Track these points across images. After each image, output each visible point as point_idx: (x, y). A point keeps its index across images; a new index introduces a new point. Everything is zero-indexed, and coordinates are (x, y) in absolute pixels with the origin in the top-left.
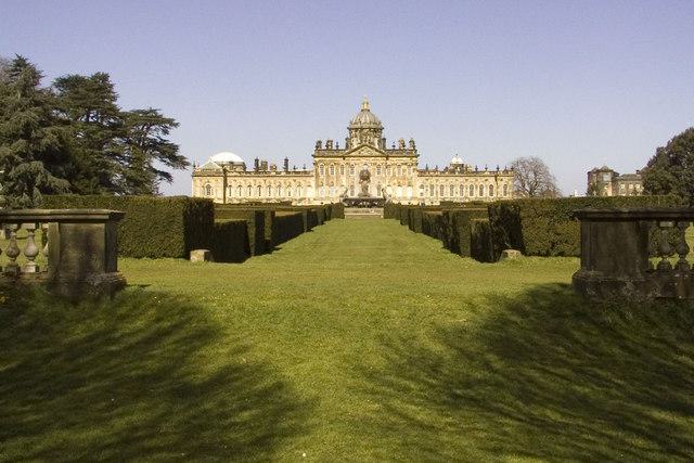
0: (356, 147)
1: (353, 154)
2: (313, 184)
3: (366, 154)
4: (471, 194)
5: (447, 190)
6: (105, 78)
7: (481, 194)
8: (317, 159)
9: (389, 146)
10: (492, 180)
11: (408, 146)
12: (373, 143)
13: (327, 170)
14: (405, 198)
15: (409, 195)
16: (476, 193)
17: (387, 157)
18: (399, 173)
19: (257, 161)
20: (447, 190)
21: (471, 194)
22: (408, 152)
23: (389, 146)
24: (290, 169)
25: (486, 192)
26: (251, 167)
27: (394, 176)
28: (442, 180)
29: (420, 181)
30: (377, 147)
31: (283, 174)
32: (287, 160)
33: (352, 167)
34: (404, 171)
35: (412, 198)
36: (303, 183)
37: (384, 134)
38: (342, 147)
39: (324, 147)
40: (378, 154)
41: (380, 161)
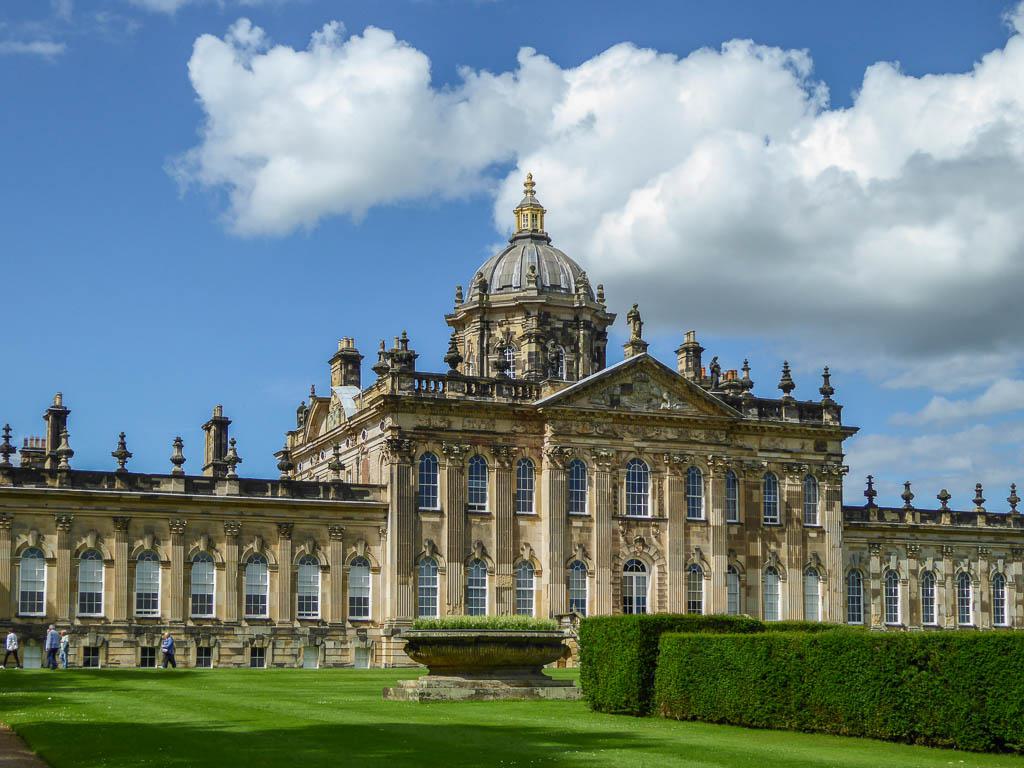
1: (583, 403)
3: (643, 409)
8: (409, 422)
17: (735, 428)
40: (690, 411)
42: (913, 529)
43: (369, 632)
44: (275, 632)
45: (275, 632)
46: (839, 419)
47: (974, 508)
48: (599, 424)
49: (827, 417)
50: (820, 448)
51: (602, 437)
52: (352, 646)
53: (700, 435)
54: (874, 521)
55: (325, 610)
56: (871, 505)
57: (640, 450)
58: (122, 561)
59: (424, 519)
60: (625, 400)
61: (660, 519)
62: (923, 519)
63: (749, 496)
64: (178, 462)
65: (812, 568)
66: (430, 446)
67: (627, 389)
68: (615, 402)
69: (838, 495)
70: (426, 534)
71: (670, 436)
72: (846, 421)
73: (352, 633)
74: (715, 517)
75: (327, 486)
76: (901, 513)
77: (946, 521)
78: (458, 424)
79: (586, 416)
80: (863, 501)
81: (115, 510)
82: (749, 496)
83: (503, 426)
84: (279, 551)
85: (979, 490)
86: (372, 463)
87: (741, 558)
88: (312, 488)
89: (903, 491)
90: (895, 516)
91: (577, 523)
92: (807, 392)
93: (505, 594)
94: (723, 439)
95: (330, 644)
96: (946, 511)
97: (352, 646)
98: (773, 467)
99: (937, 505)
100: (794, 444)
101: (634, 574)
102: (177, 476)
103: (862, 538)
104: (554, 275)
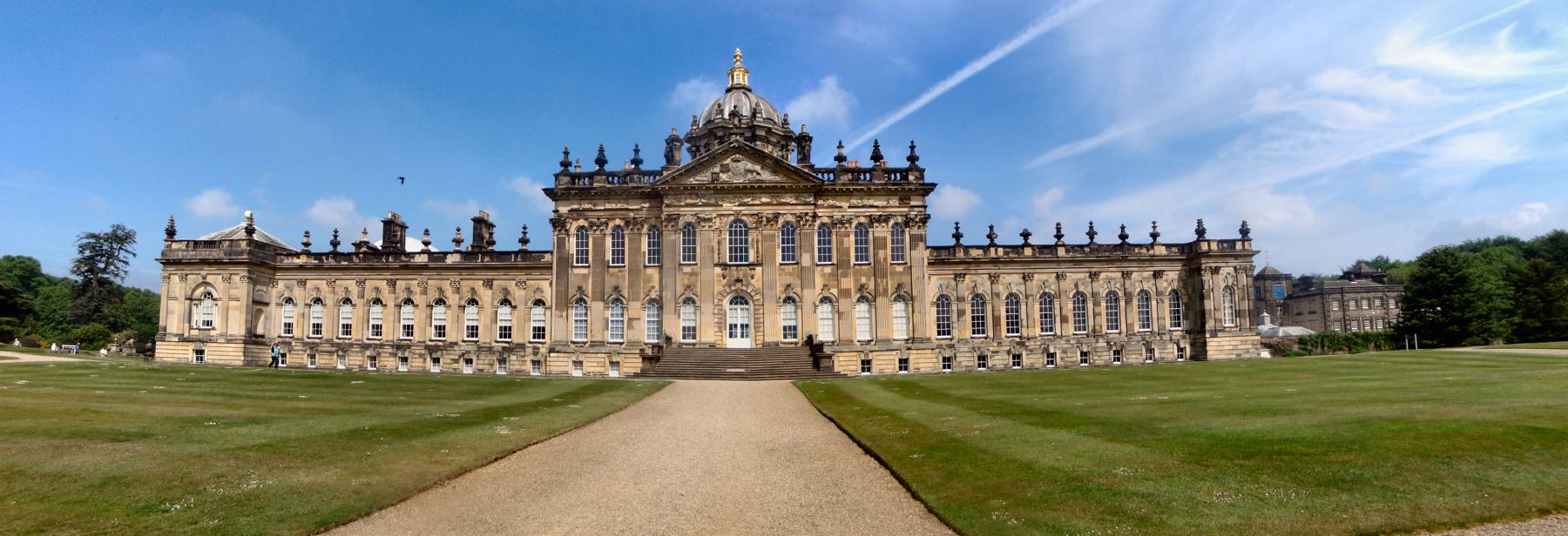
1: (692, 181)
2: (548, 294)
3: (739, 180)
5: (1032, 311)
14: (886, 345)
15: (899, 332)
17: (820, 192)
18: (862, 253)
20: (1032, 311)
27: (842, 265)
28: (1011, 280)
29: (931, 285)
31: (450, 260)
33: (690, 231)
35: (913, 341)
41: (791, 208)
42: (995, 261)
43: (543, 350)
44: (480, 349)
45: (480, 349)
46: (922, 178)
47: (1053, 241)
48: (703, 196)
49: (911, 178)
51: (705, 205)
52: (528, 359)
54: (960, 254)
55: (516, 338)
56: (958, 245)
57: (738, 213)
58: (391, 304)
59: (576, 271)
60: (724, 177)
61: (752, 266)
62: (1006, 253)
63: (840, 243)
64: (307, 244)
66: (582, 222)
67: (725, 169)
68: (715, 178)
69: (922, 238)
70: (573, 283)
71: (764, 200)
72: (927, 180)
73: (529, 350)
75: (517, 253)
76: (985, 249)
77: (1028, 252)
79: (695, 191)
80: (953, 242)
81: (388, 275)
82: (840, 243)
84: (485, 295)
85: (1058, 229)
87: (834, 291)
89: (988, 231)
90: (980, 252)
91: (687, 270)
92: (895, 159)
93: (635, 323)
94: (811, 199)
95: (513, 358)
96: (1026, 245)
97: (528, 359)
98: (863, 220)
99: (1021, 241)
101: (739, 307)
102: (423, 252)
103: (950, 271)
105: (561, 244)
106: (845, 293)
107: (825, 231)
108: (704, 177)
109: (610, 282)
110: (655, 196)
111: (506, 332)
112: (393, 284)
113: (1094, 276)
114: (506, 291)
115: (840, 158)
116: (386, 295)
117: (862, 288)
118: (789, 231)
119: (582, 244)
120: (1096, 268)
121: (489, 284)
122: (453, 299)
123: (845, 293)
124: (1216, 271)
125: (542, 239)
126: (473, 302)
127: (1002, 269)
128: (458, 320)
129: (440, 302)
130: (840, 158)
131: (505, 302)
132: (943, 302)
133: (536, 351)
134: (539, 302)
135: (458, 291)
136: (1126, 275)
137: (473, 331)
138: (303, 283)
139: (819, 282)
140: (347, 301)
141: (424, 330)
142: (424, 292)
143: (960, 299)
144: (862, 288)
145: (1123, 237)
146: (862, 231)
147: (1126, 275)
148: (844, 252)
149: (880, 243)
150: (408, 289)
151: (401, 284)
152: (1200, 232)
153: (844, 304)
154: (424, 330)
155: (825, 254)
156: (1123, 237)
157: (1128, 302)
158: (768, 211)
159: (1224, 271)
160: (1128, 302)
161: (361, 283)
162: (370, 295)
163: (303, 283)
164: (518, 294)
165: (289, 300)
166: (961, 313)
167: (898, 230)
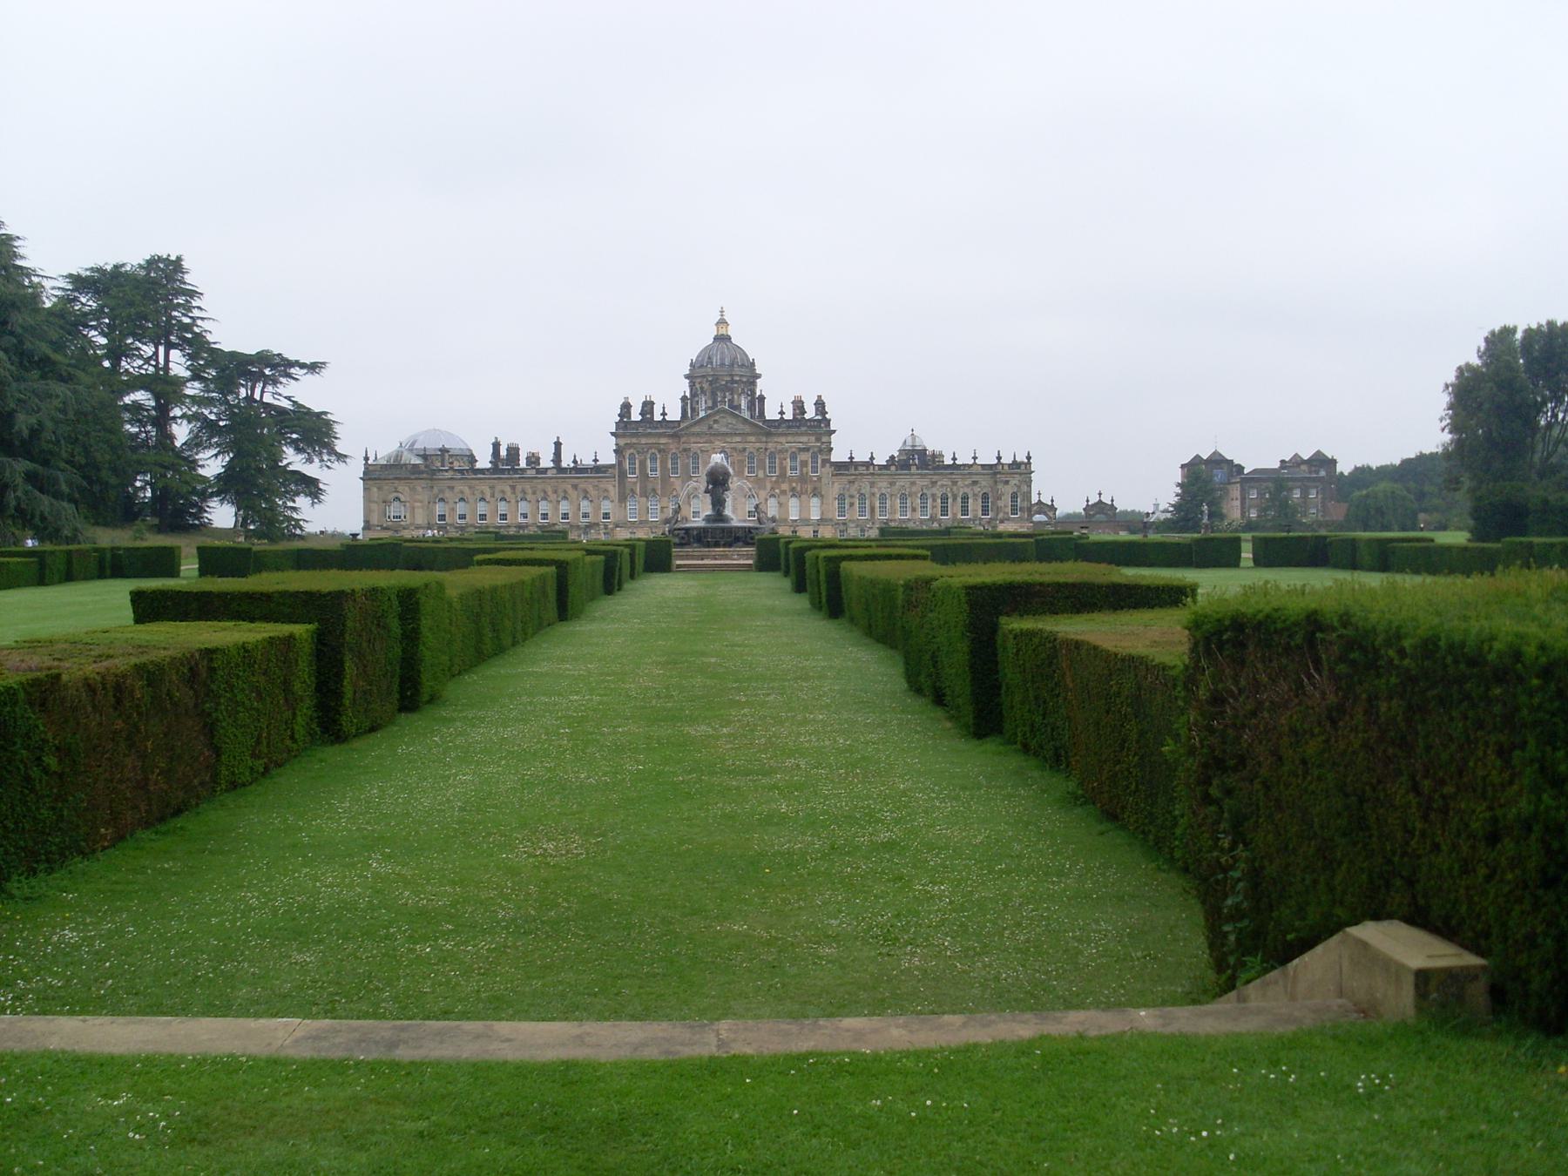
0: (702, 414)
1: (696, 429)
2: (614, 492)
3: (724, 429)
4: (944, 511)
6: (176, 266)
7: (965, 511)
8: (622, 442)
9: (771, 413)
10: (985, 483)
11: (810, 413)
12: (738, 407)
13: (643, 464)
14: (805, 521)
16: (955, 509)
17: (769, 434)
19: (496, 446)
21: (944, 511)
22: (812, 426)
23: (771, 413)
24: (566, 462)
25: (975, 506)
26: (484, 461)
27: (783, 475)
28: (883, 485)
29: (834, 488)
30: (746, 415)
31: (549, 474)
32: (558, 445)
33: (696, 457)
34: (804, 464)
35: (822, 521)
36: (590, 488)
37: (761, 387)
38: (674, 414)
39: (636, 416)
40: (747, 429)
41: (753, 444)
50: (818, 440)
53: (752, 439)
54: (852, 471)
65: (816, 493)
68: (710, 428)
70: (628, 486)
74: (761, 475)
78: (644, 441)
79: (698, 435)
83: (663, 441)
84: (573, 494)
86: (608, 458)
88: (585, 470)
100: (804, 439)
103: (845, 479)
104: (722, 359)
105: (620, 463)
106: (783, 492)
107: (772, 456)
108: (704, 428)
109: (650, 486)
110: (675, 436)
111: (586, 515)
112: (513, 488)
113: (934, 483)
114: (586, 492)
115: (782, 413)
116: (509, 495)
117: (793, 489)
118: (751, 458)
119: (632, 463)
120: (935, 478)
121: (575, 487)
122: (553, 497)
123: (783, 492)
124: (1007, 482)
125: (608, 458)
126: (565, 498)
127: (877, 479)
128: (557, 509)
129: (544, 499)
130: (782, 413)
131: (585, 497)
132: (841, 498)
133: (606, 527)
134: (606, 498)
135: (555, 492)
136: (955, 483)
137: (565, 516)
138: (452, 488)
139: (769, 486)
140: (482, 499)
141: (534, 516)
142: (534, 493)
143: (852, 497)
144: (793, 489)
145: (954, 459)
146: (793, 457)
147: (955, 483)
148: (783, 469)
149: (804, 464)
150: (524, 492)
151: (519, 488)
152: (999, 458)
153: (783, 499)
154: (534, 516)
155: (772, 469)
156: (954, 459)
157: (955, 499)
158: (740, 446)
159: (1013, 482)
160: (955, 499)
161: (492, 488)
162: (499, 496)
163: (452, 488)
164: (593, 492)
165: (442, 500)
166: (852, 505)
167: (814, 457)
